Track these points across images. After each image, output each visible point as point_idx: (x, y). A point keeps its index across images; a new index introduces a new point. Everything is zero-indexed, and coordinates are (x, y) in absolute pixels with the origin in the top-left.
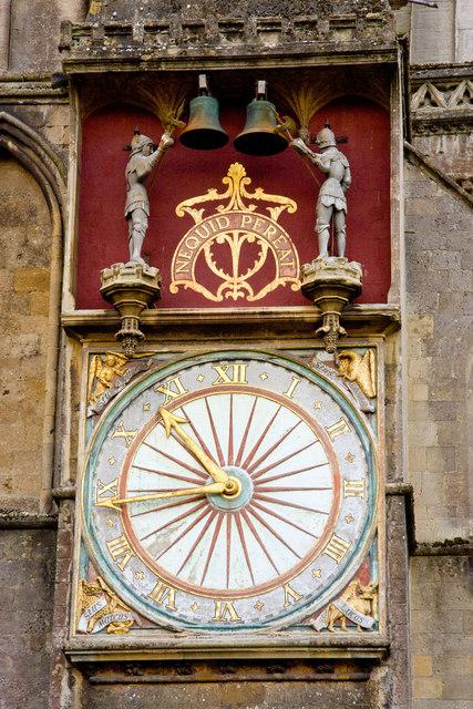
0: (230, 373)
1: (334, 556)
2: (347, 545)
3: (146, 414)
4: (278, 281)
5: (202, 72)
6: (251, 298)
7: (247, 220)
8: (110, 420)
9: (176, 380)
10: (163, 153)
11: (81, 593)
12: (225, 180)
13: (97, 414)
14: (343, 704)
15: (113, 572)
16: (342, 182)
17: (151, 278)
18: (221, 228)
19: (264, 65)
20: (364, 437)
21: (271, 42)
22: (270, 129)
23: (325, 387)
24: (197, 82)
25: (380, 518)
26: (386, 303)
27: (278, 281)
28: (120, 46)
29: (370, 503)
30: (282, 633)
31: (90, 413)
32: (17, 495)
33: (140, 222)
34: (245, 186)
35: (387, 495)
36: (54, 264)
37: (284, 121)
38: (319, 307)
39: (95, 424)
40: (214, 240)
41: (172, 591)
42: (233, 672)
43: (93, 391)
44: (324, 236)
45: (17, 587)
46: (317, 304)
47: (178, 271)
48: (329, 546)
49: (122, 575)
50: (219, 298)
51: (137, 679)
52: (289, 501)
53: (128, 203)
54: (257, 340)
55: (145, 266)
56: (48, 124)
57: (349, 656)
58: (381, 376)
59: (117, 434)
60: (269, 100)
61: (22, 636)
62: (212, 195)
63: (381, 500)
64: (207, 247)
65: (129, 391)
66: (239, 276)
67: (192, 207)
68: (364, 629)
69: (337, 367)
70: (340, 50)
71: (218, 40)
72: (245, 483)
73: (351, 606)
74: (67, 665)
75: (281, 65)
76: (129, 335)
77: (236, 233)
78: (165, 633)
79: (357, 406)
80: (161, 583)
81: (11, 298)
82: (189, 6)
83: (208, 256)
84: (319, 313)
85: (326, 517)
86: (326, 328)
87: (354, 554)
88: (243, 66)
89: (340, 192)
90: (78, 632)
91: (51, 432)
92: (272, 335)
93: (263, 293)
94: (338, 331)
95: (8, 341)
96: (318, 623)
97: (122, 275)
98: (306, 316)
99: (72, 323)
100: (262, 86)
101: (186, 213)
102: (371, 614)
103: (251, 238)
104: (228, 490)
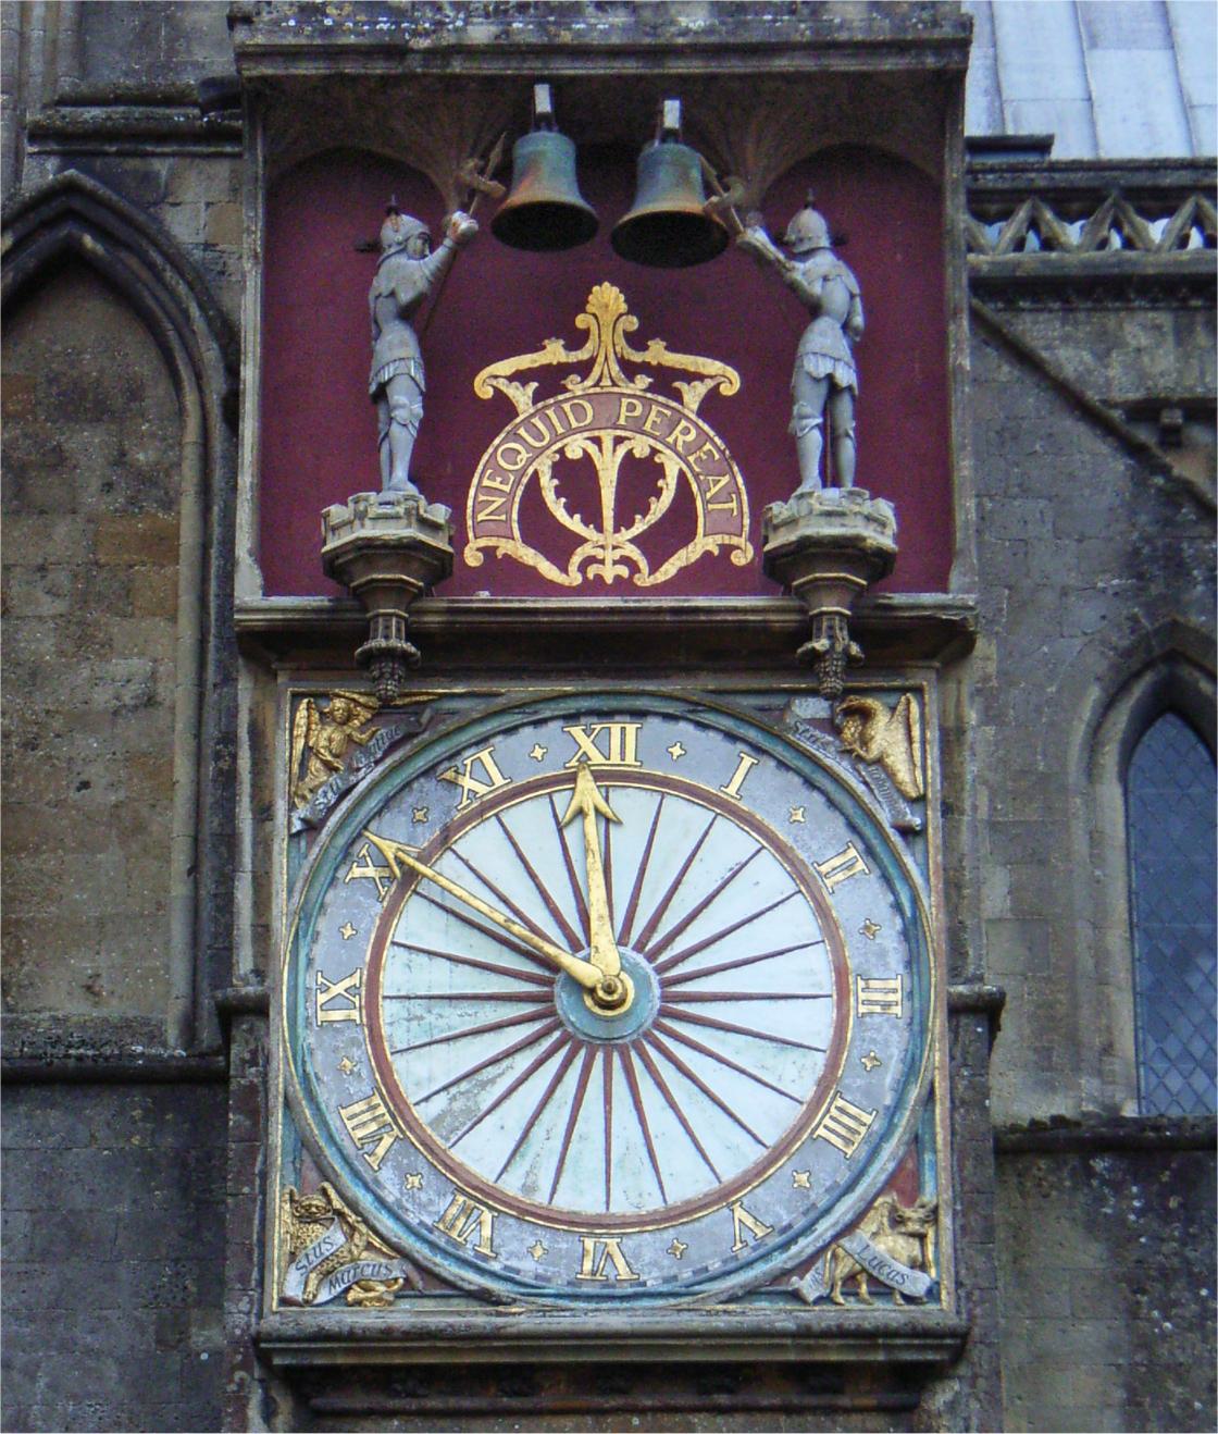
1: (838, 1142)
2: (868, 1119)
3: (420, 829)
4: (703, 544)
6: (644, 579)
7: (631, 408)
8: (341, 841)
11: (287, 1217)
12: (581, 321)
13: (312, 827)
15: (356, 1174)
16: (846, 327)
17: (433, 527)
20: (899, 886)
23: (813, 776)
25: (937, 1056)
26: (945, 590)
27: (703, 544)
29: (916, 1028)
30: (731, 1307)
31: (297, 826)
32: (114, 1009)
33: (407, 405)
35: (957, 1009)
36: (188, 505)
39: (310, 846)
40: (561, 451)
41: (487, 1216)
42: (623, 1392)
43: (302, 777)
44: (813, 442)
45: (123, 1208)
46: (801, 593)
47: (481, 517)
48: (827, 1121)
49: (376, 1181)
50: (575, 578)
51: (414, 1404)
52: (739, 1024)
53: (375, 365)
56: (171, 200)
57: (881, 1357)
58: (934, 752)
59: (357, 872)
61: (136, 1313)
62: (554, 352)
63: (938, 1022)
64: (544, 466)
66: (617, 530)
67: (511, 378)
68: (909, 1299)
69: (837, 731)
72: (642, 983)
74: (257, 1373)
76: (389, 654)
77: (607, 437)
78: (475, 1307)
79: (884, 817)
80: (461, 1199)
83: (548, 484)
84: (802, 611)
86: (821, 644)
87: (885, 1137)
89: (842, 348)
90: (284, 1301)
91: (190, 872)
93: (670, 569)
94: (846, 651)
95: (86, 673)
96: (809, 1286)
97: (378, 518)
101: (497, 391)
102: (923, 1267)
104: (601, 993)
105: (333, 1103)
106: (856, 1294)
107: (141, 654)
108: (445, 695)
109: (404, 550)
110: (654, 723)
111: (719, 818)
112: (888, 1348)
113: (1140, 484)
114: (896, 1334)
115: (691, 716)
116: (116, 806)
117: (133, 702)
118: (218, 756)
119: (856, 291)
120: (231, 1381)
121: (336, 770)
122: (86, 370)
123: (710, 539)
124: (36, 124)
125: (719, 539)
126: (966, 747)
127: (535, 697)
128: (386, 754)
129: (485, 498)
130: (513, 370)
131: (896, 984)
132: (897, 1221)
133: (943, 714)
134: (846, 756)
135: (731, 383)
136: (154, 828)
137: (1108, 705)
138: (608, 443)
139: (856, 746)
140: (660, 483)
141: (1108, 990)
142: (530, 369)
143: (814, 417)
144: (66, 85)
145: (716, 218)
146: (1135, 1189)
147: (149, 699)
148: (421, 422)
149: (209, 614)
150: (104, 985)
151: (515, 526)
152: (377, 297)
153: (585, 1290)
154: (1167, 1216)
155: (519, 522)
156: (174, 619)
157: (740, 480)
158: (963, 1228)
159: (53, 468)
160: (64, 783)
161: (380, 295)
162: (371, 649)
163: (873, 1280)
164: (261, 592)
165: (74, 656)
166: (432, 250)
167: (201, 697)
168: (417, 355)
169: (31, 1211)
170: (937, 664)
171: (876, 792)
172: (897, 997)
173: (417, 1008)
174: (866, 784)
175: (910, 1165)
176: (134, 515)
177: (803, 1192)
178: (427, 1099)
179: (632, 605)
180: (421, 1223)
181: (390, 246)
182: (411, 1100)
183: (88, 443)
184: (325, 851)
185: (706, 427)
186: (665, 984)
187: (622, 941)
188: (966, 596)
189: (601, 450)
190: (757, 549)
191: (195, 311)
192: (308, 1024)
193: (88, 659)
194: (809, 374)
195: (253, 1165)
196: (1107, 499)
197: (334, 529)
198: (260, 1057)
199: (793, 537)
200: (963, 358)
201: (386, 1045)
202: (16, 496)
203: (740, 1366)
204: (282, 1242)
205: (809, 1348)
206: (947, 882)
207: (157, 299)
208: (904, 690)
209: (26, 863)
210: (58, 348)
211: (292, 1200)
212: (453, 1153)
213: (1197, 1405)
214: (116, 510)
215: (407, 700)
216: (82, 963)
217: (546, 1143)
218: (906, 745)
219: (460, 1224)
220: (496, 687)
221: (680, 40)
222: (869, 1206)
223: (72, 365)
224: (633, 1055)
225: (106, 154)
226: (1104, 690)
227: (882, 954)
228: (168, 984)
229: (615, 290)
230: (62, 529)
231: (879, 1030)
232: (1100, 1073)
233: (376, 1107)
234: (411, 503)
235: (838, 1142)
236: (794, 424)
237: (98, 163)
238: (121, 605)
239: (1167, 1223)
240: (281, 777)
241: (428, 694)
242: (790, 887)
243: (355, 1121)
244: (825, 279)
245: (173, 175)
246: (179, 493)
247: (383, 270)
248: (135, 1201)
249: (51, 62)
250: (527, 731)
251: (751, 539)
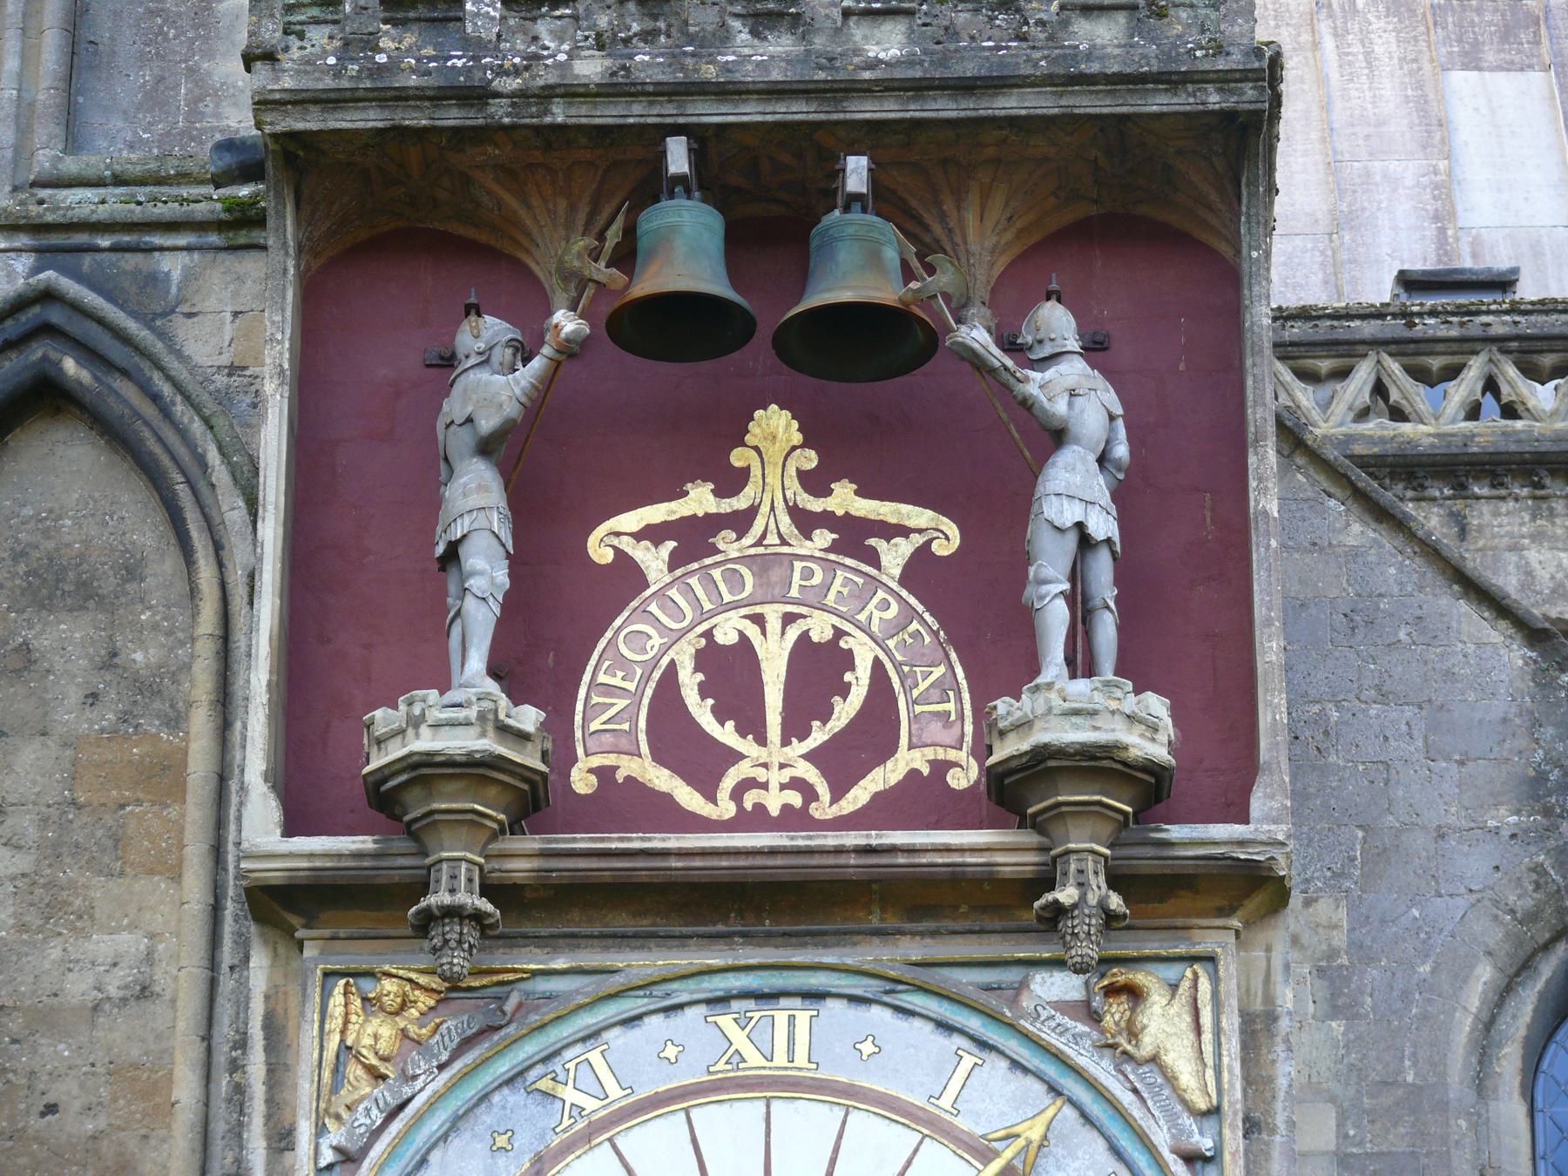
0: (762, 1037)
3: (501, 1160)
4: (906, 761)
5: (677, 130)
6: (823, 809)
7: (808, 574)
9: (595, 1057)
10: (556, 366)
12: (738, 458)
16: (1102, 460)
17: (522, 737)
18: (727, 598)
19: (866, 110)
22: (885, 291)
26: (1244, 819)
28: (429, 51)
31: (328, 1157)
34: (803, 476)
36: (201, 721)
40: (708, 634)
43: (335, 1089)
44: (1056, 618)
46: (1034, 824)
47: (595, 725)
50: (727, 809)
53: (443, 518)
54: (843, 937)
55: (504, 701)
56: (185, 308)
60: (878, 215)
62: (700, 500)
64: (684, 656)
65: (451, 1087)
66: (785, 742)
67: (638, 536)
70: (1095, 68)
71: (723, 37)
76: (453, 913)
77: (773, 614)
79: (1161, 1138)
83: (689, 681)
86: (1066, 895)
89: (1099, 487)
92: (892, 923)
93: (859, 796)
94: (1103, 905)
95: (56, 953)
97: (437, 726)
98: (1000, 858)
99: (276, 878)
100: (856, 172)
101: (618, 551)
103: (820, 628)
107: (133, 927)
109: (476, 769)
110: (833, 1006)
111: (927, 1140)
115: (887, 999)
116: (94, 1138)
117: (121, 993)
119: (1118, 410)
121: (384, 1077)
122: (67, 539)
123: (916, 753)
125: (930, 753)
126: (1278, 1039)
127: (665, 973)
128: (455, 1055)
129: (601, 700)
130: (642, 525)
133: (1246, 993)
134: (1107, 1052)
135: (947, 538)
137: (1505, 991)
138: (774, 624)
139: (1122, 1040)
140: (848, 677)
142: (665, 522)
143: (1061, 582)
144: (45, 159)
147: (144, 989)
148: (507, 595)
149: (226, 870)
151: (642, 737)
152: (448, 426)
155: (649, 733)
156: (176, 877)
159: (18, 672)
160: (23, 1106)
161: (452, 422)
162: (428, 909)
164: (278, 832)
165: (40, 930)
166: (526, 360)
167: (213, 984)
168: (503, 504)
171: (1150, 1103)
174: (1135, 1091)
176: (127, 737)
179: (801, 843)
181: (467, 357)
185: (912, 600)
188: (1273, 827)
189: (764, 633)
190: (981, 764)
191: (213, 456)
193: (60, 934)
194: (1051, 523)
196: (1500, 706)
199: (1025, 746)
200: (1266, 499)
207: (160, 440)
210: (28, 511)
214: (102, 730)
215: (485, 981)
218: (1192, 1036)
223: (46, 534)
225: (98, 250)
229: (786, 414)
234: (487, 705)
236: (1030, 591)
237: (87, 260)
238: (106, 859)
240: (305, 1090)
241: (515, 971)
245: (189, 276)
247: (457, 390)
250: (655, 1021)
251: (974, 753)
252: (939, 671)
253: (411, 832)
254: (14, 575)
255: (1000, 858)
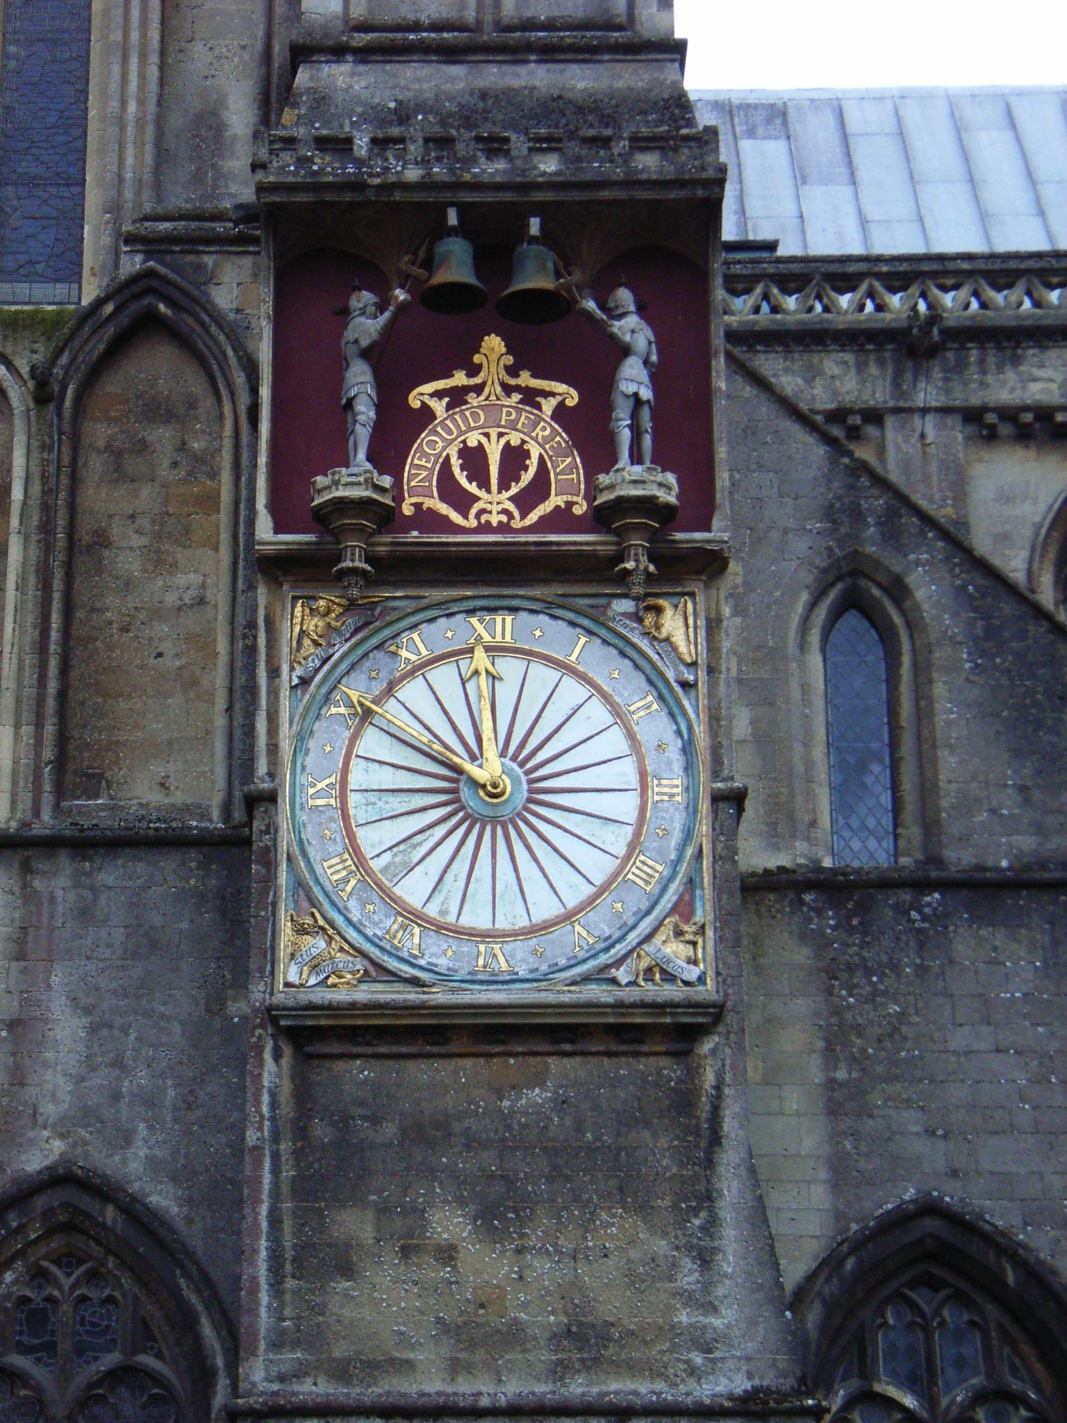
1: (641, 883)
2: (660, 868)
3: (374, 683)
4: (555, 501)
5: (452, 204)
6: (517, 524)
7: (509, 414)
8: (324, 690)
10: (395, 316)
11: (289, 931)
12: (477, 359)
13: (305, 682)
14: (657, 1085)
15: (333, 903)
16: (646, 362)
18: (473, 425)
19: (539, 196)
20: (680, 719)
21: (549, 165)
23: (626, 649)
24: (445, 217)
25: (704, 828)
26: (709, 531)
27: (555, 501)
29: (691, 810)
30: (573, 988)
31: (295, 681)
32: (178, 798)
33: (365, 412)
35: (717, 798)
36: (226, 476)
37: (570, 274)
38: (618, 535)
39: (303, 693)
40: (464, 442)
41: (417, 930)
43: (298, 650)
44: (625, 436)
45: (184, 925)
46: (617, 532)
47: (413, 484)
48: (634, 869)
49: (346, 908)
50: (473, 523)
51: (370, 1050)
52: (577, 808)
53: (345, 387)
57: (668, 1020)
58: (702, 634)
59: (334, 710)
60: (544, 245)
63: (705, 806)
64: (453, 451)
66: (499, 492)
67: (432, 395)
68: (686, 983)
69: (640, 620)
72: (516, 781)
73: (669, 949)
74: (270, 1031)
75: (562, 196)
76: (354, 571)
77: (493, 433)
78: (409, 988)
79: (670, 675)
80: (400, 919)
81: (163, 524)
82: (420, 117)
83: (456, 463)
85: (629, 830)
86: (630, 565)
87: (671, 879)
88: (508, 196)
89: (644, 375)
90: (287, 985)
91: (227, 710)
93: (533, 517)
94: (646, 569)
95: (160, 583)
96: (622, 975)
98: (599, 548)
100: (535, 226)
101: (423, 403)
102: (695, 963)
103: (515, 439)
104: (489, 788)
105: (318, 858)
106: (652, 980)
107: (196, 571)
108: (388, 598)
112: (672, 1014)
113: (833, 462)
114: (678, 1005)
116: (180, 668)
118: (245, 637)
119: (653, 339)
120: (253, 1035)
121: (320, 645)
123: (559, 498)
124: (129, 232)
125: (565, 498)
128: (352, 635)
131: (678, 782)
132: (679, 933)
136: (204, 682)
137: (813, 604)
138: (494, 437)
139: (653, 630)
140: (527, 462)
141: (813, 786)
144: (147, 208)
145: (563, 293)
146: (830, 913)
148: (375, 423)
150: (172, 782)
151: (435, 489)
153: (480, 977)
154: (851, 930)
156: (216, 549)
157: (578, 460)
158: (721, 938)
159: (140, 452)
162: (342, 569)
163: (663, 971)
167: (234, 599)
169: (126, 927)
170: (704, 578)
172: (679, 790)
173: (372, 797)
174: (659, 654)
175: (687, 898)
176: (191, 482)
177: (618, 915)
178: (378, 855)
180: (375, 935)
182: (368, 856)
183: (162, 436)
184: (313, 697)
185: (556, 427)
186: (530, 782)
187: (503, 755)
190: (590, 503)
191: (230, 352)
192: (302, 808)
194: (622, 392)
195: (267, 898)
196: (813, 472)
197: (319, 491)
198: (272, 829)
199: (612, 497)
200: (721, 381)
201: (352, 821)
202: (116, 471)
203: (578, 1026)
204: (286, 946)
205: (622, 1015)
206: (710, 717)
207: (205, 344)
208: (683, 594)
209: (122, 705)
210: (143, 376)
211: (292, 920)
212: (395, 890)
213: (870, 1051)
216: (158, 769)
217: (455, 884)
219: (399, 935)
220: (421, 592)
221: (540, 179)
222: (661, 924)
223: (151, 387)
224: (510, 827)
225: (174, 252)
226: (811, 594)
227: (669, 763)
228: (213, 782)
229: (499, 339)
230: (146, 491)
231: (667, 812)
232: (808, 839)
233: (346, 860)
234: (368, 475)
235: (641, 883)
236: (612, 424)
237: (168, 258)
239: (851, 935)
240: (285, 650)
242: (610, 720)
243: (333, 870)
244: (633, 332)
245: (216, 265)
246: (220, 469)
247: (350, 326)
248: (192, 921)
249: (138, 193)
250: (442, 621)
251: (586, 497)
252: (569, 460)
253: (332, 532)
254: (137, 406)
255: (599, 548)
